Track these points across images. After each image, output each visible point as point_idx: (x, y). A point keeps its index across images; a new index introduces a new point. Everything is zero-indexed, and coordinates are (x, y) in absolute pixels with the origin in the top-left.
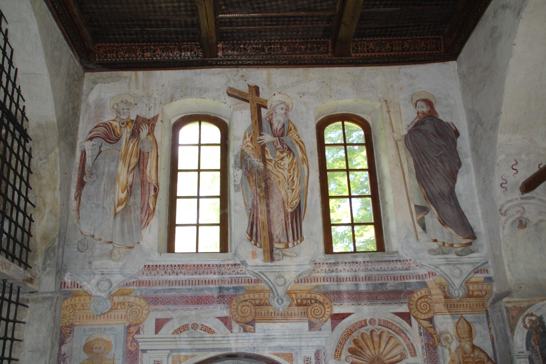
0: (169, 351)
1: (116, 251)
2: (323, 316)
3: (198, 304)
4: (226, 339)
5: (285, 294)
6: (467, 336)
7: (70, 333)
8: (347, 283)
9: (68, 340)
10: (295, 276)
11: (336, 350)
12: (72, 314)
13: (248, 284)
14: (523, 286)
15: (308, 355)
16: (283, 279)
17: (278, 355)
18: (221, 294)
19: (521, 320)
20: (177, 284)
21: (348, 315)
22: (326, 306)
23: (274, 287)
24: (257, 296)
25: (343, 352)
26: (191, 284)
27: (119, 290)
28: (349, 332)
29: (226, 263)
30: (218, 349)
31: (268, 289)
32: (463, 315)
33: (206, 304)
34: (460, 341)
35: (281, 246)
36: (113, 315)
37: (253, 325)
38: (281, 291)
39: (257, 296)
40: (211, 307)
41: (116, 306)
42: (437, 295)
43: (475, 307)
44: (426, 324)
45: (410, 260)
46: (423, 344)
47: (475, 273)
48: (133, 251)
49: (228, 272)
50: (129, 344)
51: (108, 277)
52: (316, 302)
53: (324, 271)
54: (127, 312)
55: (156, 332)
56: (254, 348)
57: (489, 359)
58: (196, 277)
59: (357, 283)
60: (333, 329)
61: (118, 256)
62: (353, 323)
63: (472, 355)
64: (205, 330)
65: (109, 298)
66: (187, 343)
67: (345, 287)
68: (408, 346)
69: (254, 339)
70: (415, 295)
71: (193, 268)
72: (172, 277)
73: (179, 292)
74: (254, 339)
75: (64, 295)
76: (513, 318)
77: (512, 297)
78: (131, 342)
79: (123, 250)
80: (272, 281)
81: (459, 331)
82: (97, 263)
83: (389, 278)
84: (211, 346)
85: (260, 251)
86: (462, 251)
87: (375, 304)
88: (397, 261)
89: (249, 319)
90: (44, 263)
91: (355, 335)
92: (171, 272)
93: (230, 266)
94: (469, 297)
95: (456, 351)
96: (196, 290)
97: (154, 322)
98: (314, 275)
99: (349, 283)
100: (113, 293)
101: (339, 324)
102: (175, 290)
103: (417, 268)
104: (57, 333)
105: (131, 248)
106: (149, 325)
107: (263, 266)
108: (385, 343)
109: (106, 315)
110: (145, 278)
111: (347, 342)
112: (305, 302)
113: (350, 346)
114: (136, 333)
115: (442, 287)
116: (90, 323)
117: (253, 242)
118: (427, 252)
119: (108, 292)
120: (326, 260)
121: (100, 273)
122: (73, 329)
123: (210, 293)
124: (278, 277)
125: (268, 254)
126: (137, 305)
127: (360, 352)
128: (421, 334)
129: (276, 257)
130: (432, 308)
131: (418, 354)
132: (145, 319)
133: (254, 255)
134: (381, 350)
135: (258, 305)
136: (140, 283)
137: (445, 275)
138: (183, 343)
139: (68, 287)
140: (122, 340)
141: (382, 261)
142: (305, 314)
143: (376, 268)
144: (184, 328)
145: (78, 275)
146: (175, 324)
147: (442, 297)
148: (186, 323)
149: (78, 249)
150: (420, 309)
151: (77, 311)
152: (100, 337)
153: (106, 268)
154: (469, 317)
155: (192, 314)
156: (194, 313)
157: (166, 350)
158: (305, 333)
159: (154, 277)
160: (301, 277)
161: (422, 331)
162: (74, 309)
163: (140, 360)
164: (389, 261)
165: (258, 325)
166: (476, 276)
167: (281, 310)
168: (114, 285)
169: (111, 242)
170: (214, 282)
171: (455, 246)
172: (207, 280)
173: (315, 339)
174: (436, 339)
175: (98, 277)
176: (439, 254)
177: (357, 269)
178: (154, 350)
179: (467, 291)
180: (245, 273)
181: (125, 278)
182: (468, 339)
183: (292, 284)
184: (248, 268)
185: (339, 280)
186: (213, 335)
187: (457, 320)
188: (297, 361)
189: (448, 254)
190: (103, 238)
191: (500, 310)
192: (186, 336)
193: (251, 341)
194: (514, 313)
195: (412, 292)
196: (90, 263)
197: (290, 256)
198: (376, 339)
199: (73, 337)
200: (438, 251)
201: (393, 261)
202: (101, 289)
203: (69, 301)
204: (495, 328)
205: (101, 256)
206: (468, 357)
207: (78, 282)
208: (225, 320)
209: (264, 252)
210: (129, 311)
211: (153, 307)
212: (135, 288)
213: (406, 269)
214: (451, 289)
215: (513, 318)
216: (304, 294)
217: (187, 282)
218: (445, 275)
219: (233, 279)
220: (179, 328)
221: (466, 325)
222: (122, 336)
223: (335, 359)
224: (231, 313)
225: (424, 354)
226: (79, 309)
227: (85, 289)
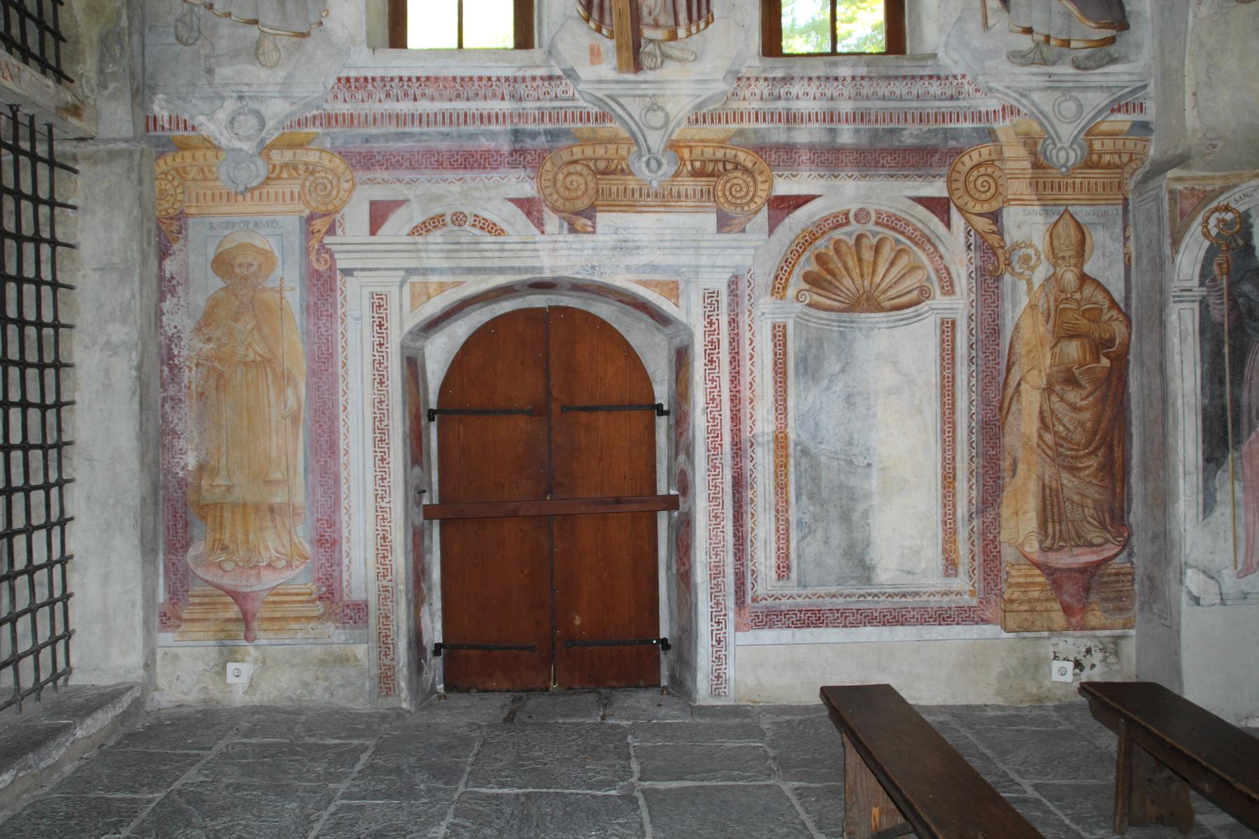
0: (402, 273)
1: (268, 44)
2: (752, 200)
3: (465, 168)
4: (530, 247)
5: (666, 147)
6: (1072, 253)
7: (179, 232)
8: (809, 125)
9: (175, 247)
10: (691, 106)
11: (776, 277)
12: (179, 190)
13: (579, 125)
14: (1220, 144)
15: (713, 286)
16: (660, 114)
17: (645, 284)
18: (518, 146)
19: (1199, 219)
20: (417, 122)
21: (808, 199)
22: (759, 179)
23: (641, 131)
24: (600, 151)
25: (792, 281)
26: (447, 121)
27: (283, 134)
28: (809, 238)
29: (529, 73)
30: (513, 268)
31: (628, 135)
32: (1070, 208)
33: (485, 168)
34: (1055, 266)
35: (660, 34)
36: (272, 191)
37: (591, 218)
38: (656, 141)
39: (600, 151)
40: (495, 175)
41: (277, 171)
42: (1018, 159)
43: (1100, 190)
44: (983, 224)
45: (964, 76)
46: (972, 268)
47: (1113, 111)
48: (309, 44)
49: (535, 94)
50: (313, 257)
51: (253, 105)
52: (736, 168)
53: (758, 97)
54: (303, 186)
55: (373, 232)
56: (593, 267)
58: (460, 105)
59: (833, 126)
60: (771, 230)
61: (275, 55)
62: (818, 217)
63: (1077, 296)
64: (482, 228)
65: (260, 154)
66: (441, 255)
67: (804, 135)
68: (937, 271)
69: (594, 249)
70: (966, 159)
71: (452, 84)
72: (404, 107)
73: (420, 141)
74: (594, 249)
75: (157, 146)
76: (1183, 214)
77: (1189, 167)
78: (318, 253)
79: (285, 41)
80: (637, 118)
81: (1056, 243)
82: (225, 72)
83: (909, 117)
84: (497, 263)
85: (608, 46)
86: (1088, 58)
87: (872, 176)
88: (931, 77)
89: (581, 204)
90: (101, 71)
91: (821, 245)
92: (401, 94)
93: (539, 82)
94: (1090, 167)
95: (1042, 285)
96: (460, 136)
97: (365, 208)
98: (735, 105)
99: (816, 125)
100: (268, 142)
101: (787, 220)
102: (412, 135)
103: (978, 95)
104: (149, 231)
105: (303, 35)
106: (356, 217)
107: (617, 82)
108: (887, 265)
109: (257, 193)
110: (341, 108)
111: (802, 259)
112: (710, 167)
113: (808, 269)
114: (326, 233)
115: (1029, 142)
116: (223, 209)
117: (592, 24)
118: (1005, 57)
119: (258, 140)
120: (765, 70)
121: (235, 95)
122: (186, 224)
123: (493, 144)
124: (654, 107)
125: (628, 55)
126: (325, 170)
127: (830, 283)
128: (969, 247)
129: (647, 62)
130: (1000, 188)
131: (957, 289)
132: (345, 202)
133: (595, 55)
134: (877, 279)
135: (603, 173)
136: (330, 120)
137: (1042, 113)
138: (432, 255)
139: (163, 128)
140: (297, 248)
141: (896, 78)
142: (711, 194)
143: (880, 94)
144: (436, 222)
145: (184, 100)
146: (415, 214)
147: (1027, 165)
148: (438, 210)
149: (177, 37)
150: (973, 191)
151: (189, 184)
152: (247, 240)
153: (247, 84)
154: (1083, 213)
155: (452, 190)
156: (456, 188)
157: (395, 269)
158: (707, 237)
159: (361, 105)
160: (704, 111)
161: (972, 240)
162: (182, 178)
163: (339, 292)
164: (913, 77)
165: (602, 218)
166: (1112, 118)
167: (655, 184)
168: (270, 124)
169: (256, 22)
170: (501, 119)
171: (1073, 44)
172: (485, 113)
173: (729, 252)
174: (1002, 259)
175: (230, 105)
176: (1033, 63)
177: (836, 94)
178: (370, 270)
179: (1086, 152)
180: (573, 99)
181: (295, 107)
182: (1073, 261)
183: (683, 126)
184: (581, 86)
185: (792, 118)
186: (501, 239)
187: (1056, 217)
188: (689, 297)
189: (1054, 64)
190: (234, 11)
191: (1157, 198)
192: (439, 239)
193: (586, 252)
194: (1187, 205)
195: (959, 152)
196: (210, 71)
197: (680, 60)
198: (867, 255)
199: (186, 240)
200: (1031, 55)
201: (922, 77)
202: (241, 132)
203: (169, 159)
204: (1137, 239)
205: (234, 55)
207: (186, 117)
208: (527, 206)
209: (619, 48)
210: (307, 183)
211: (362, 175)
212: (319, 130)
213: (952, 98)
214: (1051, 147)
215: (1183, 214)
216: (711, 150)
217: (440, 117)
218: (1042, 113)
219: (546, 113)
220: (424, 223)
221: (1073, 230)
222: (296, 240)
223: (772, 295)
224: (541, 189)
225: (970, 290)
226: (194, 180)
227: (204, 133)
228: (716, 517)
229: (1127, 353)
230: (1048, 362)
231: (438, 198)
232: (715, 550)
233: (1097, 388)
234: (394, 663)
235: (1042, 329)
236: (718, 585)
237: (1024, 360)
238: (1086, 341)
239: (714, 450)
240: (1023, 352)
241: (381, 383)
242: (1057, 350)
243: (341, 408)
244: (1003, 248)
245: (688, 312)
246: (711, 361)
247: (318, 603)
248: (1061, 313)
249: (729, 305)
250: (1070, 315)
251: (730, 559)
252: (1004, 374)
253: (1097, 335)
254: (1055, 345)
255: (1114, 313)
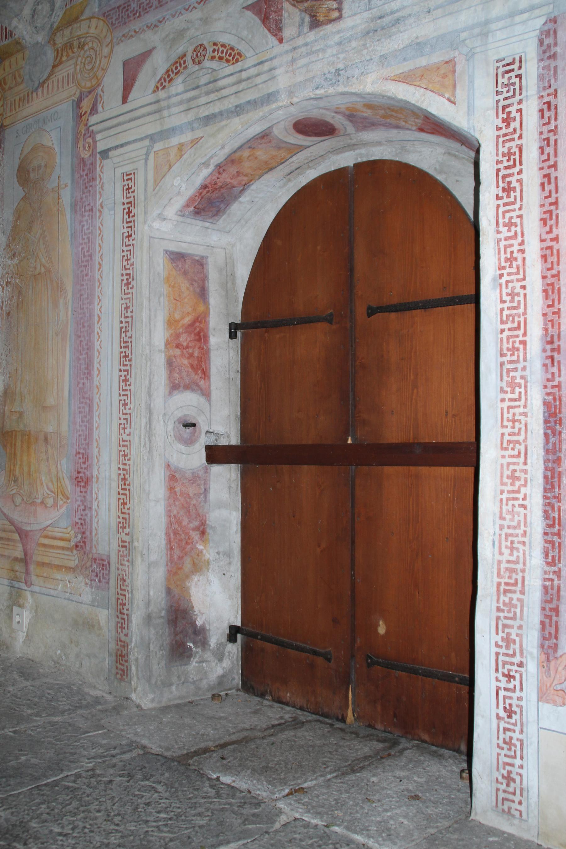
0: (147, 142)
17: (405, 78)
56: (338, 72)
65: (49, 42)
74: (340, 43)
100: (55, 25)
138: (175, 110)
144: (178, 66)
146: (159, 63)
148: (180, 50)
193: (329, 51)
228: (513, 478)
231: (181, 33)
232: (510, 540)
234: (127, 640)
236: (510, 605)
239: (514, 349)
241: (128, 284)
243: (96, 318)
245: (470, 111)
246: (508, 190)
247: (75, 552)
249: (541, 77)
251: (536, 559)
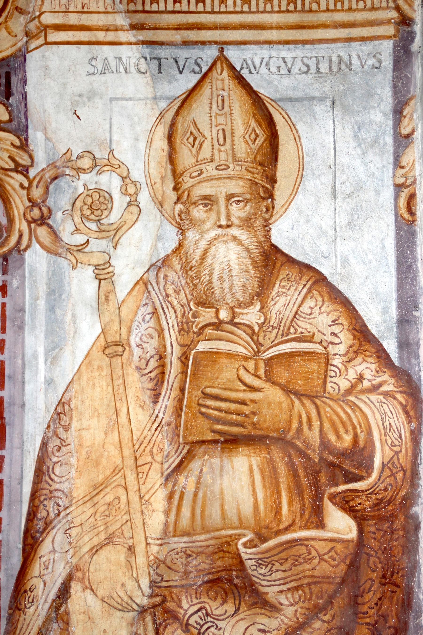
32: (233, 54)
57: (363, 337)
63: (252, 316)
81: (186, 157)
95: (143, 282)
174: (19, 203)
182: (238, 212)
187: (189, 80)
206: (218, 325)
221: (240, 118)
229: (409, 500)
230: (156, 521)
233: (316, 611)
235: (140, 418)
237: (80, 514)
238: (277, 455)
240: (79, 487)
242: (187, 481)
244: (24, 171)
248: (195, 365)
250: (227, 373)
252: (17, 560)
253: (313, 436)
254: (179, 468)
255: (367, 368)
